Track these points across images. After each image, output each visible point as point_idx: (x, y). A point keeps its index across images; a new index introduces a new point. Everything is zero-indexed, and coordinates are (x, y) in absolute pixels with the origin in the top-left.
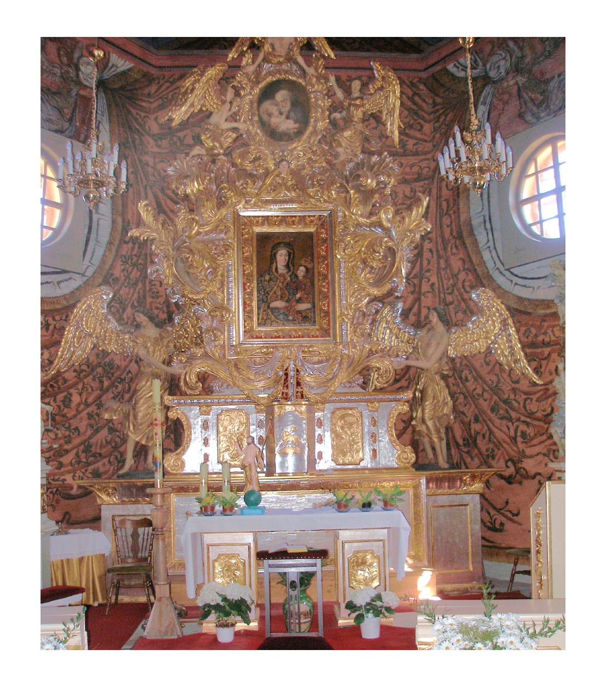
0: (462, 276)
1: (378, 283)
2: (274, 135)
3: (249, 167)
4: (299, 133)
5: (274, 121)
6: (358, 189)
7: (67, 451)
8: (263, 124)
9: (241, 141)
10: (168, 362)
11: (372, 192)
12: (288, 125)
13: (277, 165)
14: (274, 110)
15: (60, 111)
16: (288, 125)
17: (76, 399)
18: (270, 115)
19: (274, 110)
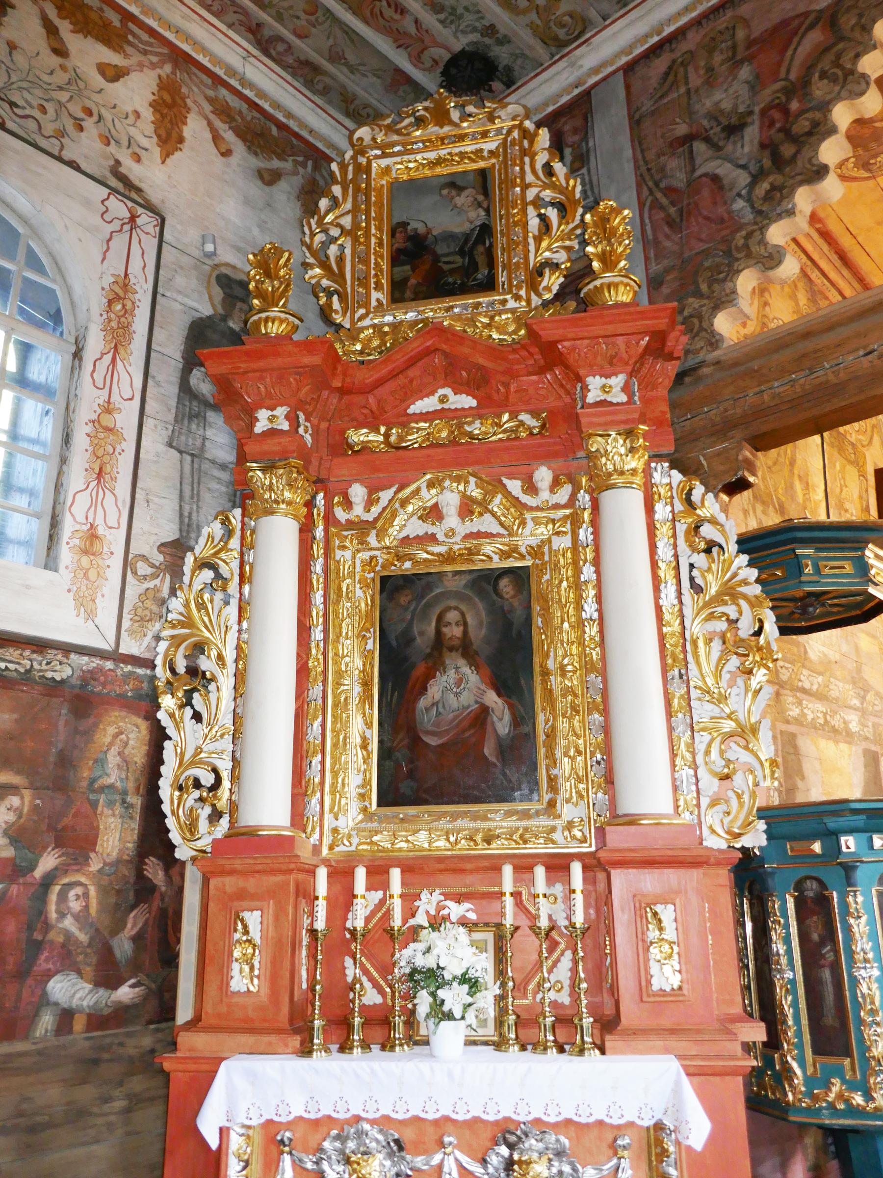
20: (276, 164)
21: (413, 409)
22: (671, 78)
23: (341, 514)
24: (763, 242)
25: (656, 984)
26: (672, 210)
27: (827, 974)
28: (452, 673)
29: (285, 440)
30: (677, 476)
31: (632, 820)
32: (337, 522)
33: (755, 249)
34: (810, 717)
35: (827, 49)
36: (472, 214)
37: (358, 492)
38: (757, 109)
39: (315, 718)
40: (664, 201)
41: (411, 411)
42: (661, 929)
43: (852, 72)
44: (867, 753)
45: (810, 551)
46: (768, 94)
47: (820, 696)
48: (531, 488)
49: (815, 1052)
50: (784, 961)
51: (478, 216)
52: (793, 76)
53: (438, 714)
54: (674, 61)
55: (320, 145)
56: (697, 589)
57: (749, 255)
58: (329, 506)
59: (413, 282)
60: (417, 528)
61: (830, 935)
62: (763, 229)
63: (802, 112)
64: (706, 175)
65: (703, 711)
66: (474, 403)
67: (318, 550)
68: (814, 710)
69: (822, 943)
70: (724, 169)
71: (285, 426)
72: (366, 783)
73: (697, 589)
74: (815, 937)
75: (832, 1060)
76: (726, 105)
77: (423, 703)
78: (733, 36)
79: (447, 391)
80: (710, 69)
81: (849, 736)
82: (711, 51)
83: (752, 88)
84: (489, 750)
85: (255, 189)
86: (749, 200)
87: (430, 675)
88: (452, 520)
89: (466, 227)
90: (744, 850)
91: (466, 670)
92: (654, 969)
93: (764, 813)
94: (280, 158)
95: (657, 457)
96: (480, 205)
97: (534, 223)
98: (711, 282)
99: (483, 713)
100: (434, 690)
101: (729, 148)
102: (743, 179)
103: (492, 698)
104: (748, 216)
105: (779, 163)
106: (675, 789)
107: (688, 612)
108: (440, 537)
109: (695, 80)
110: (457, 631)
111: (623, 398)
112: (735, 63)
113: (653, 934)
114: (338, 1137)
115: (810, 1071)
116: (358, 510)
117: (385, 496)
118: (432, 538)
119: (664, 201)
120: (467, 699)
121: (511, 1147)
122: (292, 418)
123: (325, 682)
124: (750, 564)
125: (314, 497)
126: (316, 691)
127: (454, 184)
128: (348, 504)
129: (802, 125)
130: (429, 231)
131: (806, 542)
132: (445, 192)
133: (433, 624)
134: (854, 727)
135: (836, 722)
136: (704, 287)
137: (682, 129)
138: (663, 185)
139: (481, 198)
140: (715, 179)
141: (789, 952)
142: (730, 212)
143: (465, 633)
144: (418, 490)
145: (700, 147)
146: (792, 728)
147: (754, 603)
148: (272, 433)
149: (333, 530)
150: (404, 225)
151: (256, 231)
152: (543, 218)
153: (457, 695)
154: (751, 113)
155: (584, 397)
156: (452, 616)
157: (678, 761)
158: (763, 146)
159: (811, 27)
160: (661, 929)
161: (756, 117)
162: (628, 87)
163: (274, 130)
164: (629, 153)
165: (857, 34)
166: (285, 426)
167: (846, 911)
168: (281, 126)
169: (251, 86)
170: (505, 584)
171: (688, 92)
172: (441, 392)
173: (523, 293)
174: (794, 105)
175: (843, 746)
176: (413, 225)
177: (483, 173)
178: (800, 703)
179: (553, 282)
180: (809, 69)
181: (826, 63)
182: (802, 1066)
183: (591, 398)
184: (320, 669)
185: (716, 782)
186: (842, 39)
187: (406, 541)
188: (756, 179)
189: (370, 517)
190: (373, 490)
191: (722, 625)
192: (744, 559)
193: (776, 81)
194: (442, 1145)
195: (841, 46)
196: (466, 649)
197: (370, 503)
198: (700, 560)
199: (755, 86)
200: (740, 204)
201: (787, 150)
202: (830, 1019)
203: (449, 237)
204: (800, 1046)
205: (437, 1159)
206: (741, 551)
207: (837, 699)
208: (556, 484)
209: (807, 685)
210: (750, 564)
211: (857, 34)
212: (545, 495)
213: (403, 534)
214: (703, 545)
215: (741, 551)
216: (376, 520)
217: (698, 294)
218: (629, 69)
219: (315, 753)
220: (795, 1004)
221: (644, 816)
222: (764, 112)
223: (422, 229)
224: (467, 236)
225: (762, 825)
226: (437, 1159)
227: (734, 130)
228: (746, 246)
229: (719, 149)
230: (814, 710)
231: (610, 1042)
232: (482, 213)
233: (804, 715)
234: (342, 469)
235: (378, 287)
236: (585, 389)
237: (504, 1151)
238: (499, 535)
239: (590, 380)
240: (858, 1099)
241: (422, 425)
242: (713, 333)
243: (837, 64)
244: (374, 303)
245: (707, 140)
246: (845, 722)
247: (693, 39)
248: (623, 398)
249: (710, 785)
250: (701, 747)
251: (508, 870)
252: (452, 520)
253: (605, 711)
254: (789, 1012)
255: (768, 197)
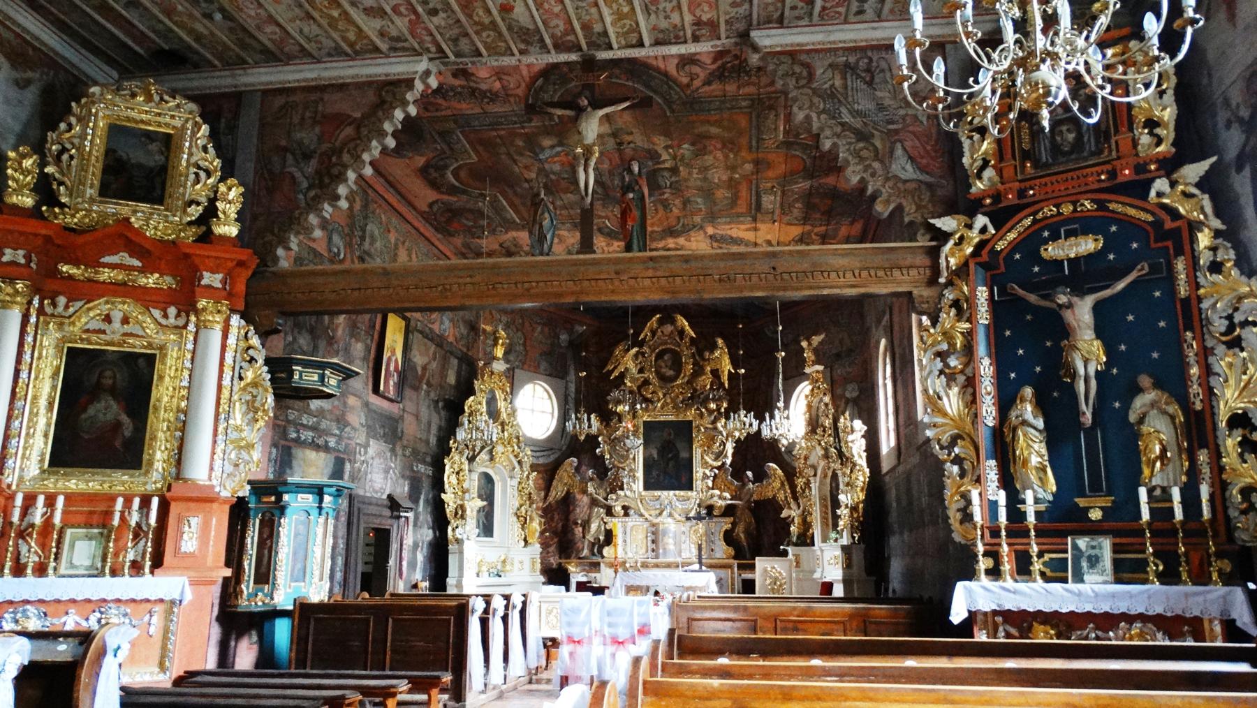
0: (768, 452)
1: (716, 459)
2: (663, 379)
3: (650, 396)
4: (676, 378)
5: (664, 370)
6: (706, 409)
7: (551, 546)
8: (658, 373)
9: (646, 382)
10: (606, 499)
11: (714, 411)
12: (671, 373)
13: (664, 395)
14: (663, 364)
15: (551, 364)
16: (671, 373)
17: (556, 517)
18: (661, 367)
19: (663, 364)
20: (30, 74)
21: (102, 260)
22: (284, 111)
23: (49, 310)
24: (306, 219)
25: (183, 549)
26: (270, 183)
27: (266, 552)
28: (103, 403)
29: (23, 270)
30: (243, 322)
31: (186, 480)
32: (45, 314)
33: (302, 220)
34: (303, 438)
35: (354, 139)
36: (157, 158)
37: (62, 300)
38: (319, 152)
39: (17, 418)
40: (266, 176)
41: (102, 260)
42: (190, 527)
43: (359, 157)
44: (337, 458)
45: (299, 368)
46: (325, 146)
47: (313, 428)
48: (166, 316)
49: (255, 583)
50: (249, 546)
51: (160, 159)
52: (338, 144)
53: (92, 423)
54: (287, 103)
55: (60, 61)
56: (241, 378)
57: (299, 224)
58: (41, 303)
59: (114, 186)
60: (97, 324)
61: (271, 536)
62: (308, 214)
63: (338, 164)
64: (289, 173)
65: (233, 435)
66: (140, 264)
67: (30, 329)
68: (307, 435)
69: (267, 539)
70: (298, 175)
71: (23, 261)
72: (43, 455)
73: (241, 378)
74: (265, 536)
75: (260, 586)
76: (306, 141)
77: (83, 416)
78: (317, 107)
79: (126, 255)
80: (303, 119)
81: (326, 448)
82: (306, 108)
83: (319, 139)
84: (118, 443)
85: (13, 93)
86: (305, 196)
87: (91, 402)
88: (116, 324)
89: (152, 164)
90: (238, 497)
91: (112, 402)
92: (183, 543)
93: (249, 482)
94: (32, 69)
95: (233, 311)
96: (162, 154)
97: (192, 177)
98: (280, 229)
99: (117, 425)
100: (91, 411)
101: (302, 165)
102: (305, 184)
103: (125, 418)
104: (303, 204)
105: (322, 186)
106: (211, 469)
107: (236, 388)
108: (108, 332)
109: (296, 120)
110: (110, 382)
111: (220, 286)
112: (315, 122)
113: (186, 528)
114: (12, 612)
115: (251, 590)
116: (60, 309)
117: (79, 304)
118: (104, 332)
119: (266, 176)
120: (109, 417)
121: (101, 613)
122: (28, 258)
123: (25, 400)
124: (268, 372)
125: (32, 300)
126: (19, 404)
127: (150, 136)
128: (54, 305)
129: (335, 171)
130: (129, 159)
131: (297, 365)
132: (143, 139)
133: (97, 375)
134: (332, 444)
135: (321, 442)
136: (276, 231)
137: (283, 143)
138: (269, 167)
139: (163, 149)
140: (293, 178)
141: (252, 543)
142: (296, 198)
143: (114, 383)
144: (99, 304)
145: (289, 157)
146: (291, 444)
147: (266, 390)
148: (13, 263)
149: (42, 318)
150: (115, 151)
151: (9, 120)
152: (197, 174)
153: (105, 414)
154: (315, 152)
155: (199, 281)
156: (108, 373)
157: (215, 457)
158: (318, 172)
159: (350, 124)
160: (190, 527)
161: (317, 155)
162: (262, 102)
163: (31, 52)
164: (255, 141)
165: (365, 140)
166: (23, 261)
167: (280, 525)
168: (34, 48)
169: (19, 25)
170: (141, 361)
171: (290, 124)
172: (121, 254)
173: (178, 214)
174: (334, 159)
175: (322, 454)
176: (120, 153)
177: (169, 135)
178: (298, 432)
179: (195, 212)
180: (344, 144)
181: (351, 145)
182: (248, 588)
183: (203, 282)
184: (23, 393)
185: (232, 467)
186: (359, 138)
187: (87, 331)
188: (309, 189)
189: (67, 315)
190: (71, 300)
191: (249, 397)
192: (266, 369)
193: (330, 142)
194: (67, 613)
195: (358, 142)
196: (113, 392)
197: (67, 307)
198: (245, 365)
199: (320, 139)
200: (301, 196)
201: (327, 180)
202: (263, 569)
203: (140, 166)
204: (248, 581)
205: (63, 620)
206: (265, 364)
207: (324, 430)
208: (178, 316)
209: (305, 422)
210: (268, 372)
211: (365, 140)
212: (172, 321)
213: (86, 327)
214: (248, 358)
215: (265, 364)
216: (70, 317)
217: (273, 234)
218: (266, 93)
219: (14, 437)
220: (250, 565)
221: (190, 480)
222: (321, 155)
223: (124, 155)
224: (151, 170)
225: (248, 487)
226: (63, 620)
227: (307, 156)
228: (299, 218)
229: (298, 163)
230: (307, 435)
231: (156, 571)
232: (163, 159)
233: (300, 438)
234: (50, 285)
235: (92, 186)
236: (201, 277)
237: (98, 615)
238: (142, 337)
239: (204, 273)
240: (267, 601)
241: (106, 270)
242: (276, 255)
243: (355, 149)
244: (88, 196)
245: (293, 154)
246: (326, 442)
247: (297, 98)
248: (220, 286)
249: (229, 468)
250: (228, 451)
251: (120, 501)
252: (116, 324)
253: (183, 430)
254: (247, 571)
255: (313, 199)
